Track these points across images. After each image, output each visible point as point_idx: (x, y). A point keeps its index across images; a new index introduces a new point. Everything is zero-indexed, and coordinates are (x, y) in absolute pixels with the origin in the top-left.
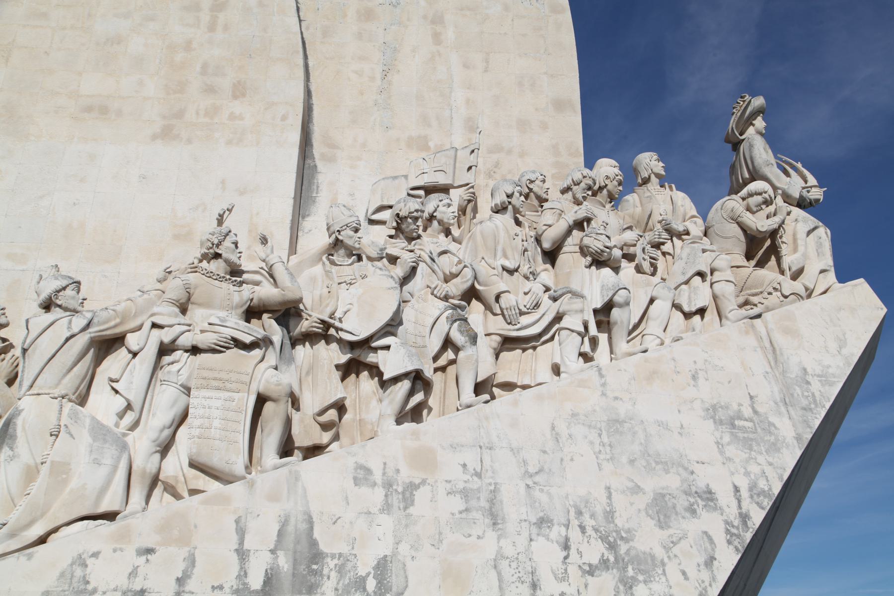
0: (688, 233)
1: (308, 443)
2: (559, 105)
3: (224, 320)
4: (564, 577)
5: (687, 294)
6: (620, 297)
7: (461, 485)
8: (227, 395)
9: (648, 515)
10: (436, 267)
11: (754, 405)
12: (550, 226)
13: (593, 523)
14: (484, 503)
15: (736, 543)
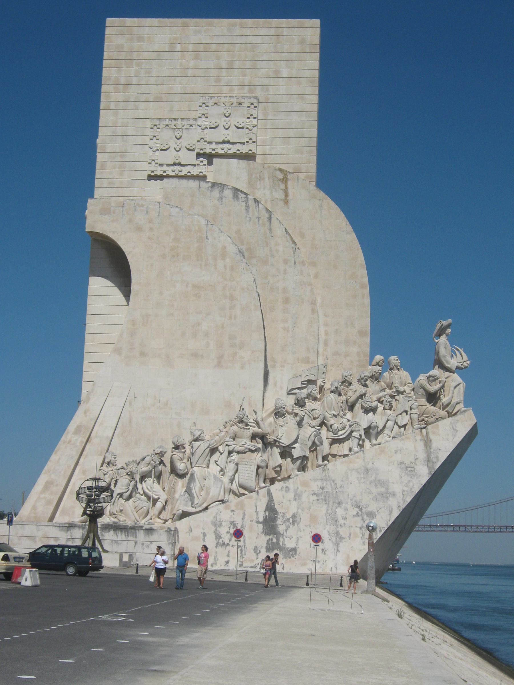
0: (405, 391)
1: (271, 477)
2: (361, 333)
3: (246, 442)
4: (345, 519)
5: (400, 418)
6: (373, 425)
7: (316, 492)
8: (249, 466)
9: (373, 499)
10: (311, 415)
11: (416, 462)
12: (350, 397)
13: (355, 503)
14: (323, 497)
15: (400, 508)
